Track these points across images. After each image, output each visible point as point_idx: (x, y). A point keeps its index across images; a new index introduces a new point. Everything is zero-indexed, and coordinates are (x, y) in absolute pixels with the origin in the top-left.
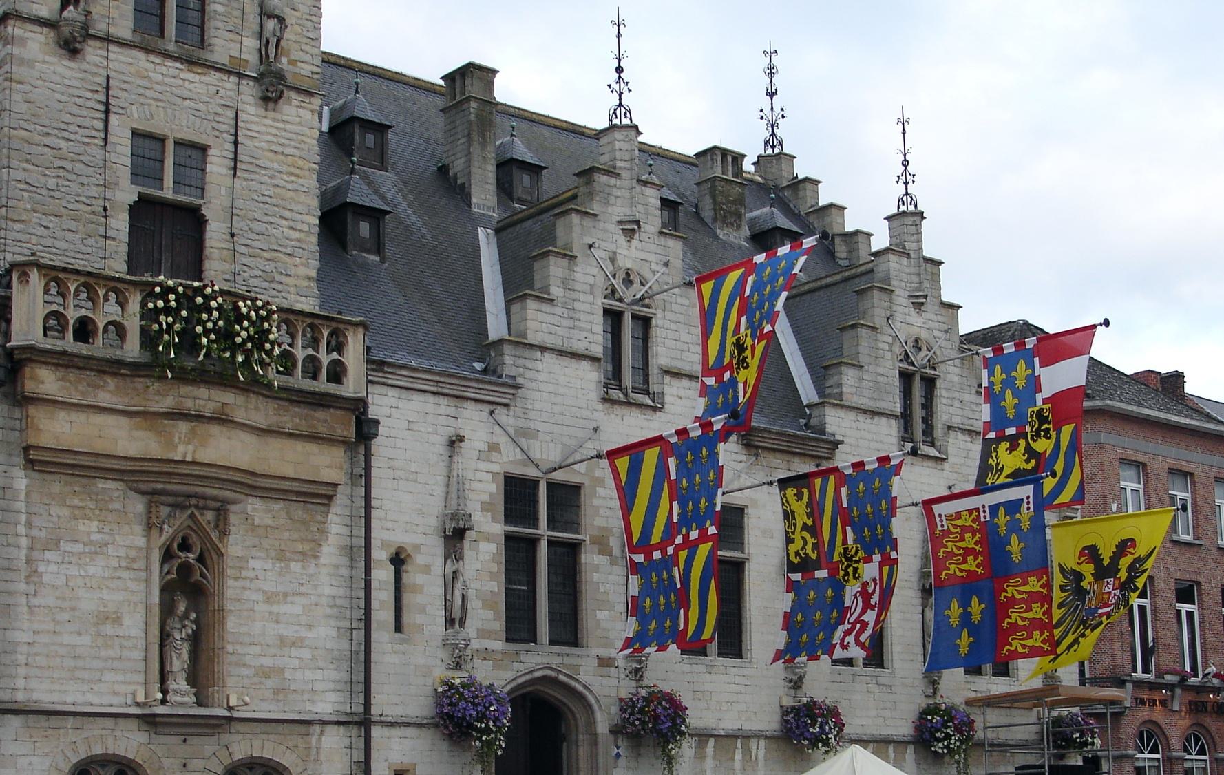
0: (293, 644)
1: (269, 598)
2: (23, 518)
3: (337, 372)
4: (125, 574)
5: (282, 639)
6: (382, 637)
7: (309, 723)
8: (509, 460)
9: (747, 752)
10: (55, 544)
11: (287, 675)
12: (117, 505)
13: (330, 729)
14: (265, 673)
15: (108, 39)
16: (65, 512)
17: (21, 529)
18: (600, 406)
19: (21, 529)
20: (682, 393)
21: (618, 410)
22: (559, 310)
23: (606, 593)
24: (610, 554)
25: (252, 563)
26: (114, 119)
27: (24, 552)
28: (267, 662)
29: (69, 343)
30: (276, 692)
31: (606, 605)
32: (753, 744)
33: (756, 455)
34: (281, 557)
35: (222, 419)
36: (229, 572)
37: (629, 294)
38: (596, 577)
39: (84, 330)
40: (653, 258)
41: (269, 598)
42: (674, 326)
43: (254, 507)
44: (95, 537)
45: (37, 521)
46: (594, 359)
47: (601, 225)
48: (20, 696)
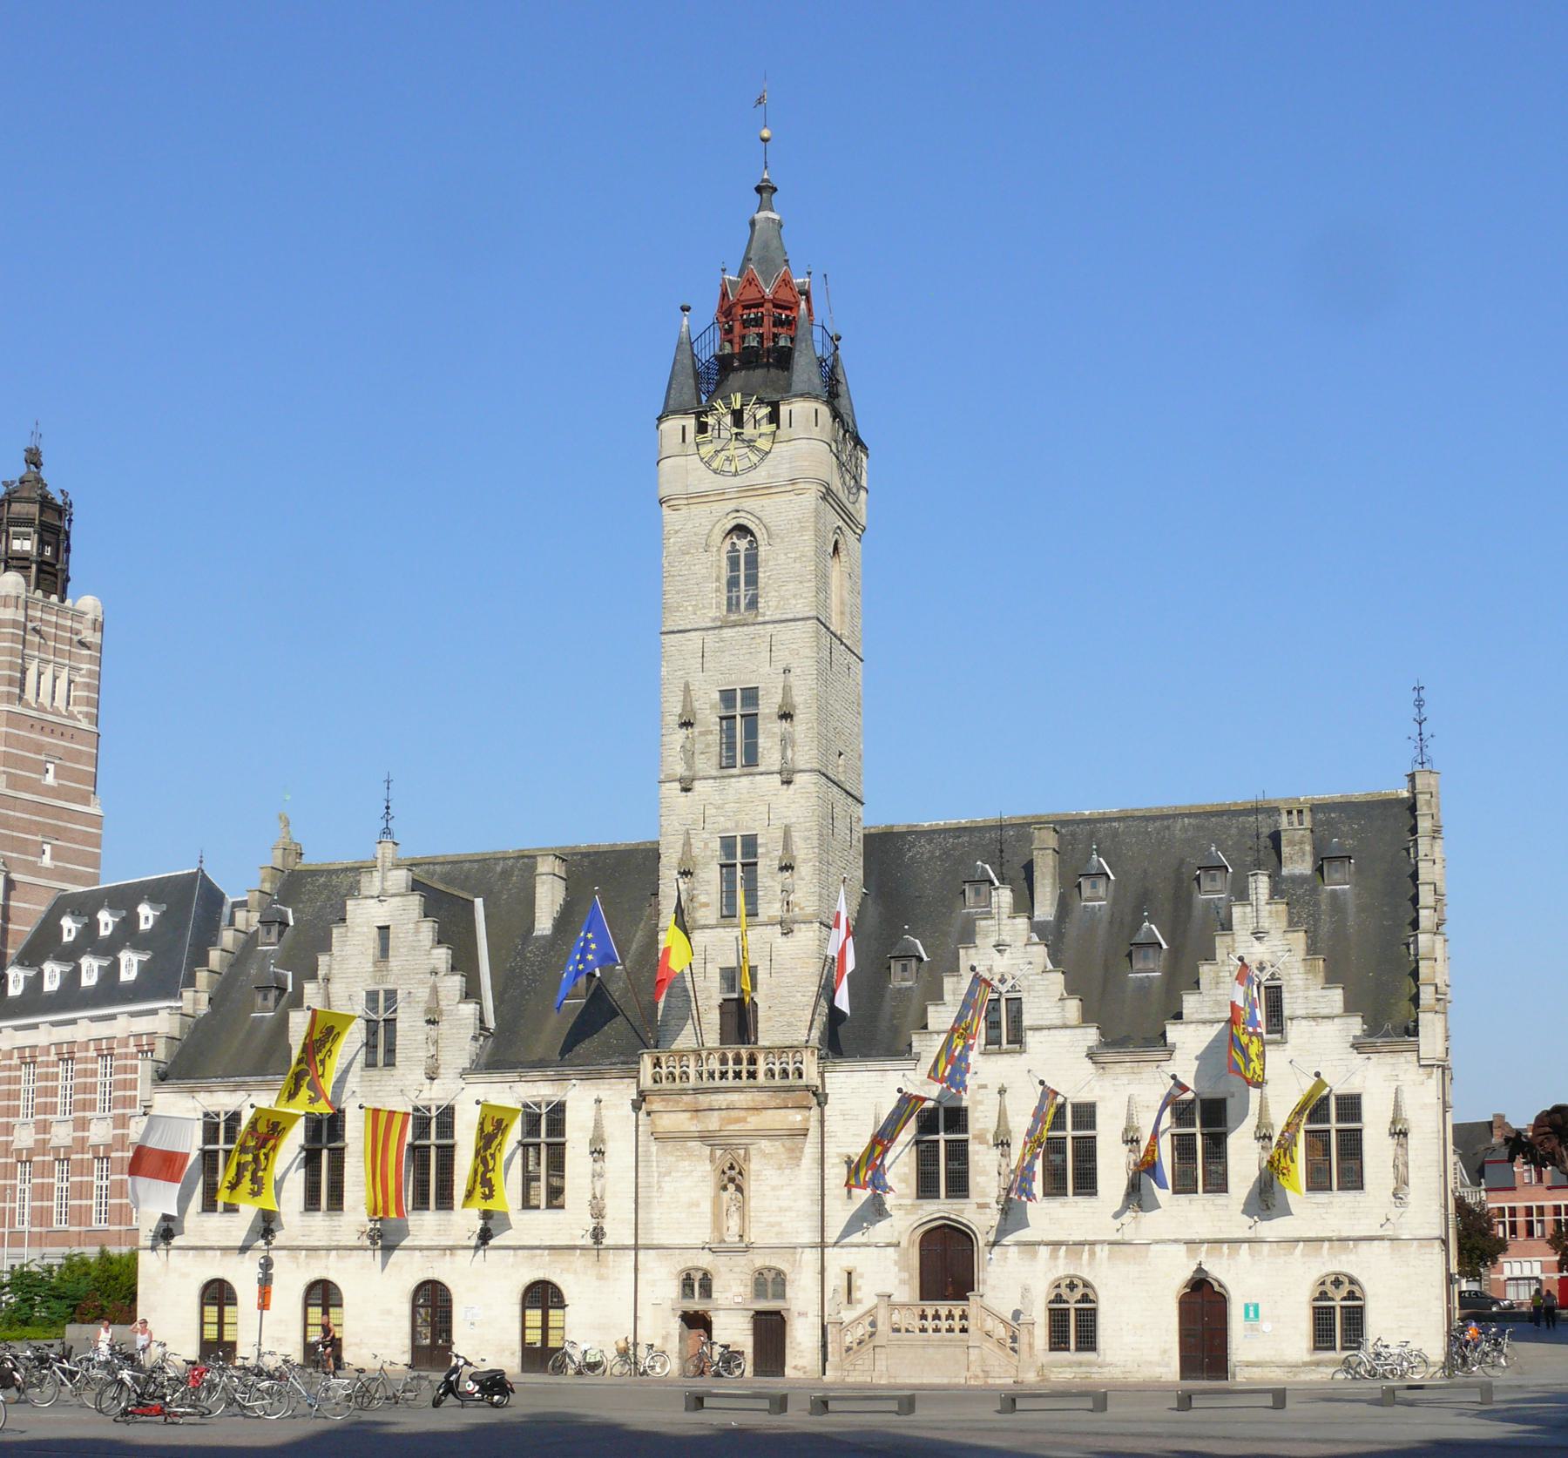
0: (786, 1210)
1: (774, 1188)
2: (655, 1164)
4: (701, 1184)
9: (1092, 1254)
10: (668, 1173)
11: (784, 1225)
12: (697, 1153)
16: (674, 1159)
17: (654, 1169)
19: (654, 1169)
20: (1042, 1039)
21: (993, 1058)
22: (950, 1009)
23: (984, 1166)
24: (987, 1143)
25: (765, 1172)
26: (708, 965)
27: (656, 1179)
28: (772, 1220)
29: (665, 1085)
30: (777, 1234)
31: (984, 1173)
32: (1098, 1248)
33: (1103, 1068)
36: (752, 1178)
37: (1003, 989)
40: (1021, 961)
42: (1037, 1000)
43: (765, 1144)
44: (687, 1168)
45: (661, 1164)
47: (981, 951)
48: (655, 1242)
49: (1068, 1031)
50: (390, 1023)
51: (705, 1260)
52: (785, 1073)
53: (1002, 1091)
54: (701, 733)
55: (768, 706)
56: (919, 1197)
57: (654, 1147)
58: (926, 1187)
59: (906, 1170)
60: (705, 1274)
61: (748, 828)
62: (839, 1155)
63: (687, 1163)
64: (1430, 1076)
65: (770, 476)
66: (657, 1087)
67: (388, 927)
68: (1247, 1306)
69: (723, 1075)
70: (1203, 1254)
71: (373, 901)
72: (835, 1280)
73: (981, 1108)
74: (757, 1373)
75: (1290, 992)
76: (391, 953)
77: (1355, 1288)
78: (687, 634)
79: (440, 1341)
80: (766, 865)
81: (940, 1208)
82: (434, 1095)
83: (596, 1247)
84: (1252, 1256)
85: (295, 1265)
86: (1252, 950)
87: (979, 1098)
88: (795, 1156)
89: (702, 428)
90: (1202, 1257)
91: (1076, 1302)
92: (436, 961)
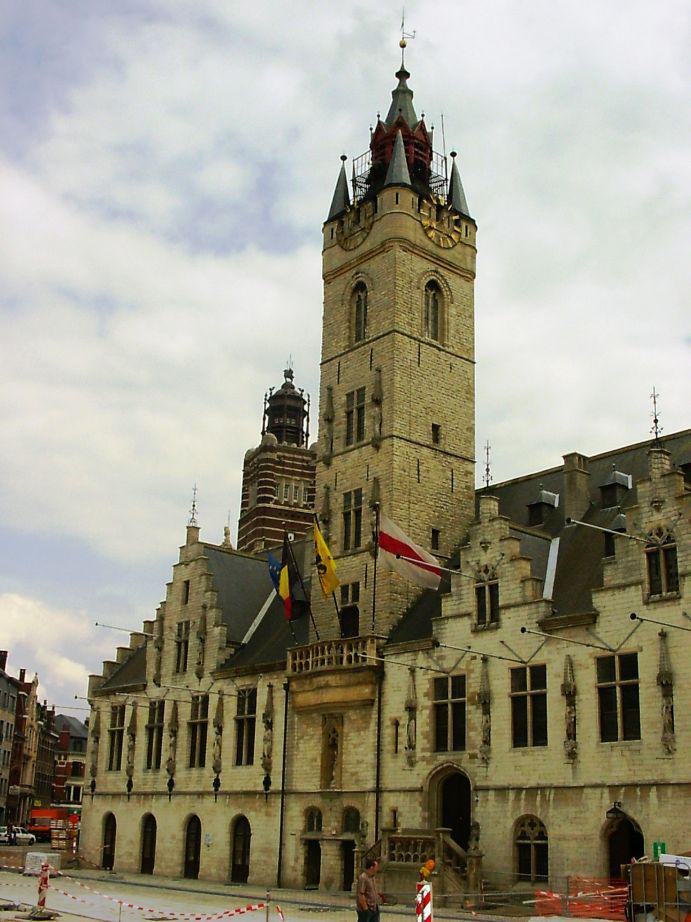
6: (387, 757)
7: (364, 792)
10: (302, 738)
13: (372, 794)
14: (353, 774)
18: (472, 636)
28: (353, 770)
31: (474, 729)
34: (358, 730)
35: (327, 686)
37: (485, 577)
38: (469, 716)
41: (355, 746)
43: (352, 715)
46: (469, 615)
49: (527, 608)
50: (186, 643)
53: (485, 660)
54: (337, 425)
56: (435, 751)
58: (439, 745)
60: (320, 813)
61: (358, 484)
62: (390, 719)
65: (371, 245)
70: (622, 797)
73: (472, 675)
75: (682, 551)
80: (365, 507)
82: (202, 687)
86: (652, 519)
87: (471, 667)
88: (366, 720)
90: (621, 799)
91: (537, 839)
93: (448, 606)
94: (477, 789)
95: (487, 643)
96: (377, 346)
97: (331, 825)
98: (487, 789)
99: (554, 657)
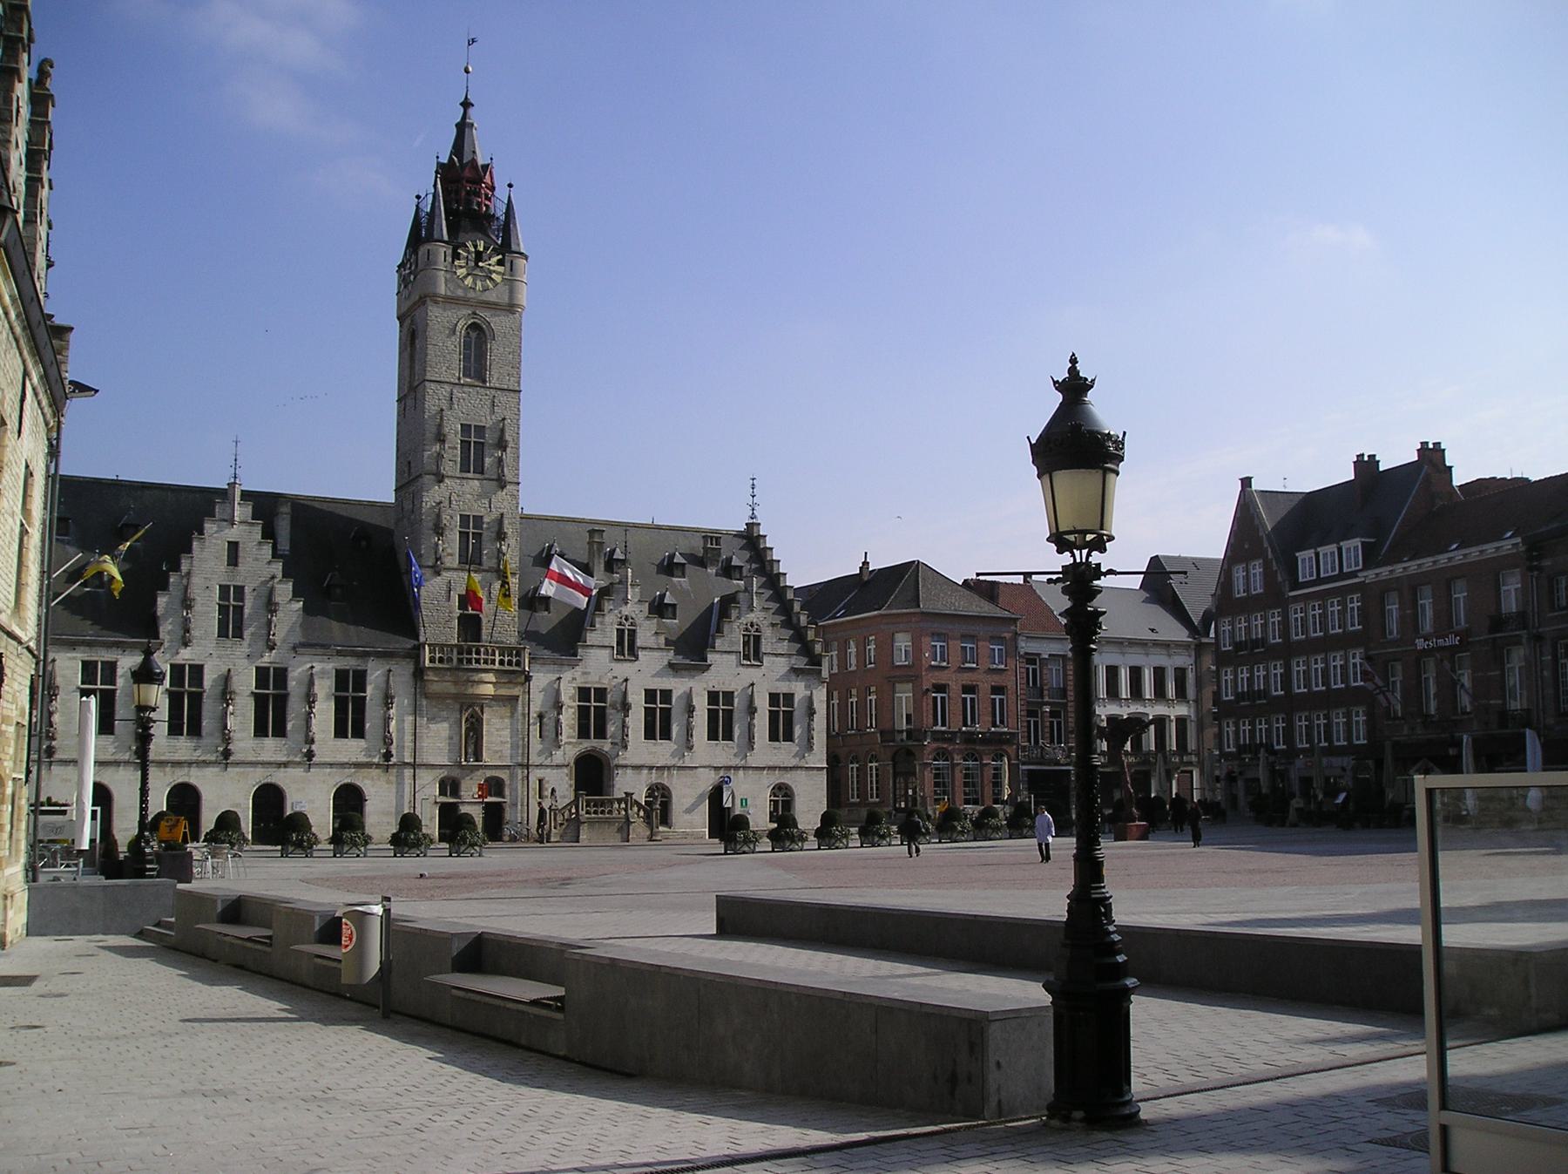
3: (518, 664)
5: (502, 742)
8: (580, 682)
14: (497, 752)
15: (449, 569)
29: (437, 665)
39: (441, 660)
51: (456, 773)
52: (510, 663)
55: (490, 438)
57: (424, 703)
58: (583, 733)
59: (573, 722)
63: (445, 713)
64: (824, 687)
66: (431, 665)
67: (236, 544)
68: (742, 800)
69: (478, 661)
71: (225, 523)
72: (534, 785)
74: (710, 838)
76: (240, 560)
77: (788, 791)
78: (442, 385)
79: (272, 825)
81: (591, 743)
83: (224, 762)
84: (744, 774)
85: (162, 774)
89: (456, 256)
92: (275, 570)
93: (591, 637)
94: (617, 766)
95: (624, 669)
96: (502, 398)
97: (470, 790)
98: (626, 766)
99: (678, 686)
